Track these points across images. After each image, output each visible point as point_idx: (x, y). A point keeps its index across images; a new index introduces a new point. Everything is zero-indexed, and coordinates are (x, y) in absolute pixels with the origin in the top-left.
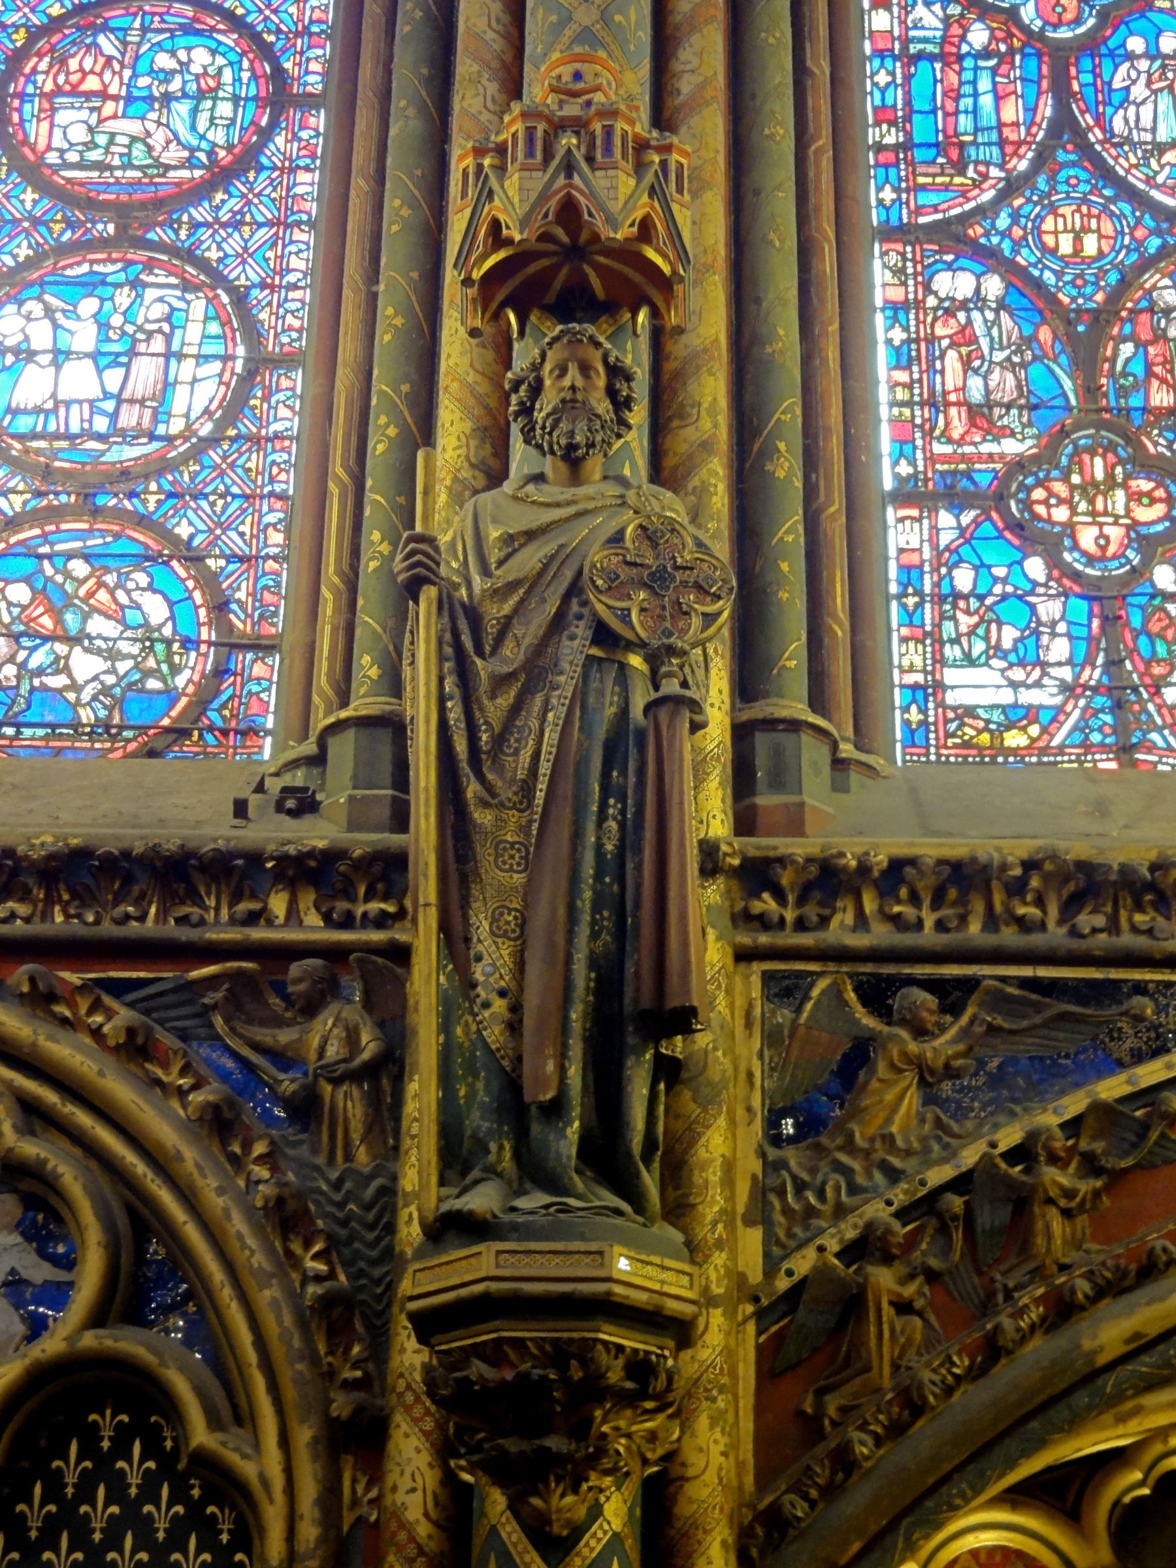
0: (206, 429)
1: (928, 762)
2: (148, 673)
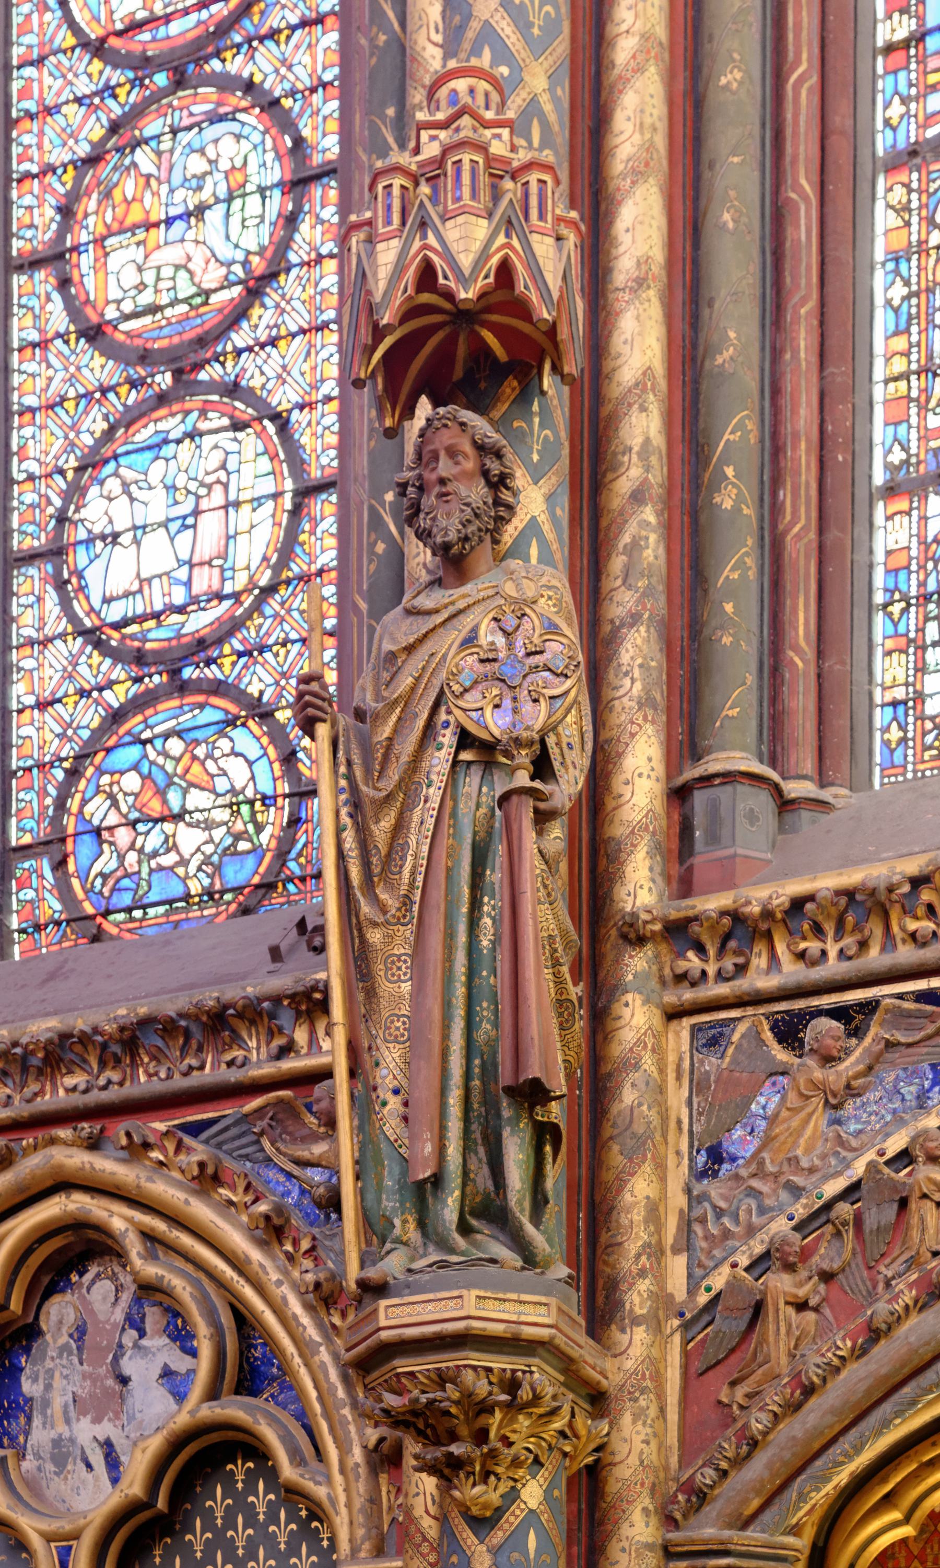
0: (264, 581)
1: (906, 780)
2: (238, 837)
